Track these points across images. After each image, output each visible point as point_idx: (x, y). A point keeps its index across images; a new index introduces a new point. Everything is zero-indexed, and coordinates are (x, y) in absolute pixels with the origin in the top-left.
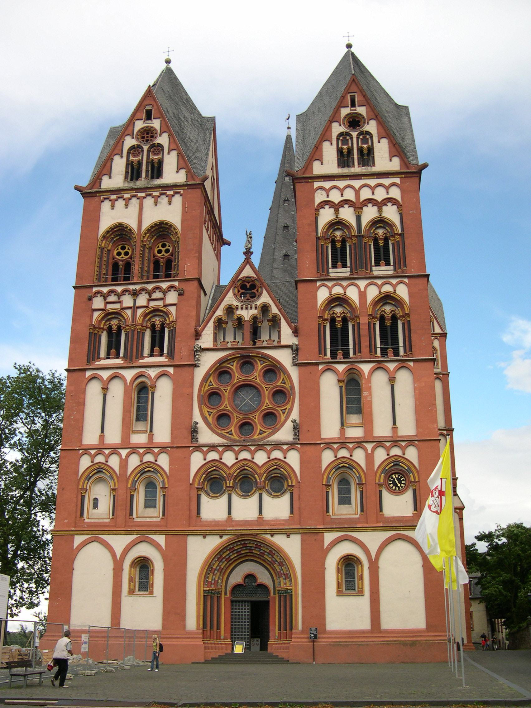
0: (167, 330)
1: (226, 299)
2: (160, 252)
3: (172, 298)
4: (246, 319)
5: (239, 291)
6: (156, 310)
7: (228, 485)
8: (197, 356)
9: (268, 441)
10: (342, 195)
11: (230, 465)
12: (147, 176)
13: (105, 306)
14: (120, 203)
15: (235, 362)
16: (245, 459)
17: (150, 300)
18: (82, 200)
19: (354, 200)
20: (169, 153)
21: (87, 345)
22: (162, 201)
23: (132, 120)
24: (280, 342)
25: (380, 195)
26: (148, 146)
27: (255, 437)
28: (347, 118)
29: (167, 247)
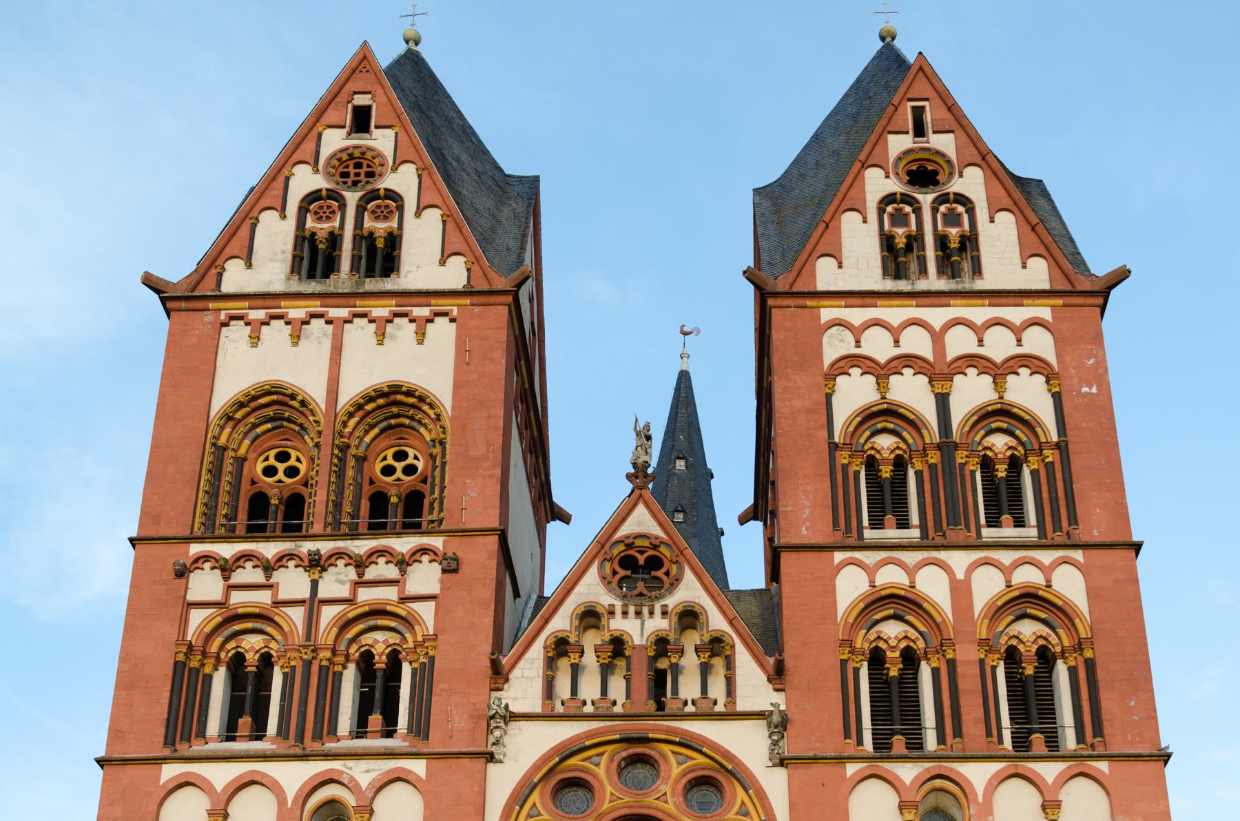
0: (406, 670)
1: (579, 589)
3: (425, 578)
4: (637, 641)
5: (615, 573)
6: (378, 611)
8: (497, 733)
10: (897, 342)
12: (354, 267)
13: (227, 595)
14: (277, 333)
15: (606, 756)
17: (358, 584)
19: (929, 355)
20: (418, 214)
21: (167, 695)
24: (735, 703)
25: (999, 346)
26: (358, 195)
28: (904, 162)
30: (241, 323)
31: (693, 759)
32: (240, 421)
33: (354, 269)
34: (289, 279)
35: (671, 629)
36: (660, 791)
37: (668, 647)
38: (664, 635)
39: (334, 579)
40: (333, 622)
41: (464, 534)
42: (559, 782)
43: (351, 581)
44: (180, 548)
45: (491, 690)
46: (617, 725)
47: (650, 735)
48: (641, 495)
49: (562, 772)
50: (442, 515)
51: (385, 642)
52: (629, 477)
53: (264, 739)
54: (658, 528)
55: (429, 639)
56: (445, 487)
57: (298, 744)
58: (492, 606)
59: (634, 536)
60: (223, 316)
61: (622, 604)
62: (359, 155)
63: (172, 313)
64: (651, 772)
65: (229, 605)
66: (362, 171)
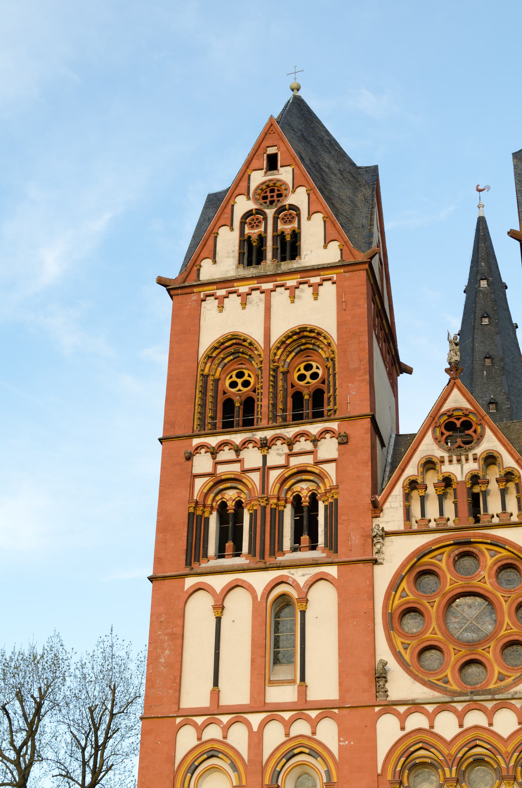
0: (321, 506)
1: (421, 448)
2: (302, 377)
4: (459, 479)
5: (442, 434)
6: (302, 471)
7: (448, 775)
8: (378, 546)
9: (516, 693)
11: (449, 737)
12: (274, 256)
13: (215, 469)
16: (476, 727)
17: (289, 456)
18: (169, 302)
20: (309, 218)
21: (185, 534)
22: (302, 294)
23: (246, 171)
26: (274, 210)
27: (492, 686)
29: (314, 370)
30: (213, 298)
31: (500, 553)
32: (215, 357)
33: (274, 257)
34: (238, 268)
35: (480, 469)
36: (481, 575)
37: (479, 481)
38: (476, 473)
39: (276, 453)
40: (277, 480)
41: (350, 419)
42: (418, 573)
43: (286, 454)
44: (185, 442)
45: (373, 518)
46: (451, 535)
47: (472, 540)
48: (455, 383)
49: (420, 566)
50: (336, 407)
51: (308, 488)
52: (447, 371)
53: (241, 555)
54: (467, 403)
55: (334, 488)
56: (336, 389)
57: (262, 560)
58: (370, 464)
59: (452, 410)
60: (202, 296)
61: (448, 455)
62: (272, 185)
63: (174, 297)
64: (475, 561)
65: (217, 474)
66: (275, 194)
